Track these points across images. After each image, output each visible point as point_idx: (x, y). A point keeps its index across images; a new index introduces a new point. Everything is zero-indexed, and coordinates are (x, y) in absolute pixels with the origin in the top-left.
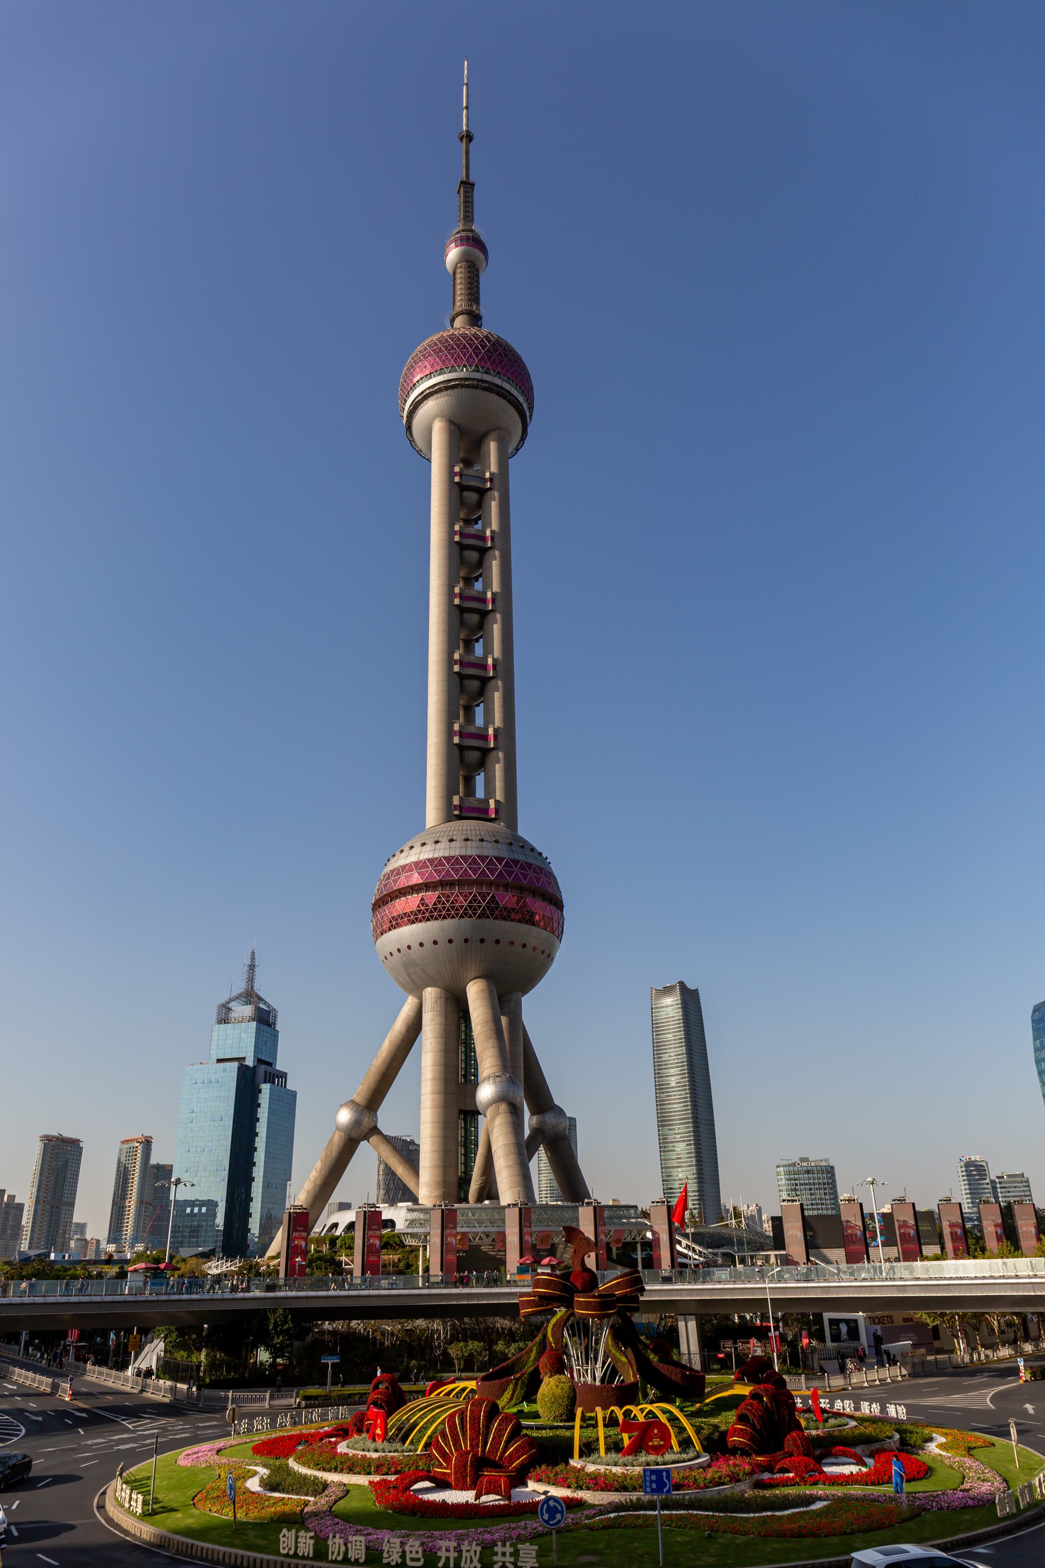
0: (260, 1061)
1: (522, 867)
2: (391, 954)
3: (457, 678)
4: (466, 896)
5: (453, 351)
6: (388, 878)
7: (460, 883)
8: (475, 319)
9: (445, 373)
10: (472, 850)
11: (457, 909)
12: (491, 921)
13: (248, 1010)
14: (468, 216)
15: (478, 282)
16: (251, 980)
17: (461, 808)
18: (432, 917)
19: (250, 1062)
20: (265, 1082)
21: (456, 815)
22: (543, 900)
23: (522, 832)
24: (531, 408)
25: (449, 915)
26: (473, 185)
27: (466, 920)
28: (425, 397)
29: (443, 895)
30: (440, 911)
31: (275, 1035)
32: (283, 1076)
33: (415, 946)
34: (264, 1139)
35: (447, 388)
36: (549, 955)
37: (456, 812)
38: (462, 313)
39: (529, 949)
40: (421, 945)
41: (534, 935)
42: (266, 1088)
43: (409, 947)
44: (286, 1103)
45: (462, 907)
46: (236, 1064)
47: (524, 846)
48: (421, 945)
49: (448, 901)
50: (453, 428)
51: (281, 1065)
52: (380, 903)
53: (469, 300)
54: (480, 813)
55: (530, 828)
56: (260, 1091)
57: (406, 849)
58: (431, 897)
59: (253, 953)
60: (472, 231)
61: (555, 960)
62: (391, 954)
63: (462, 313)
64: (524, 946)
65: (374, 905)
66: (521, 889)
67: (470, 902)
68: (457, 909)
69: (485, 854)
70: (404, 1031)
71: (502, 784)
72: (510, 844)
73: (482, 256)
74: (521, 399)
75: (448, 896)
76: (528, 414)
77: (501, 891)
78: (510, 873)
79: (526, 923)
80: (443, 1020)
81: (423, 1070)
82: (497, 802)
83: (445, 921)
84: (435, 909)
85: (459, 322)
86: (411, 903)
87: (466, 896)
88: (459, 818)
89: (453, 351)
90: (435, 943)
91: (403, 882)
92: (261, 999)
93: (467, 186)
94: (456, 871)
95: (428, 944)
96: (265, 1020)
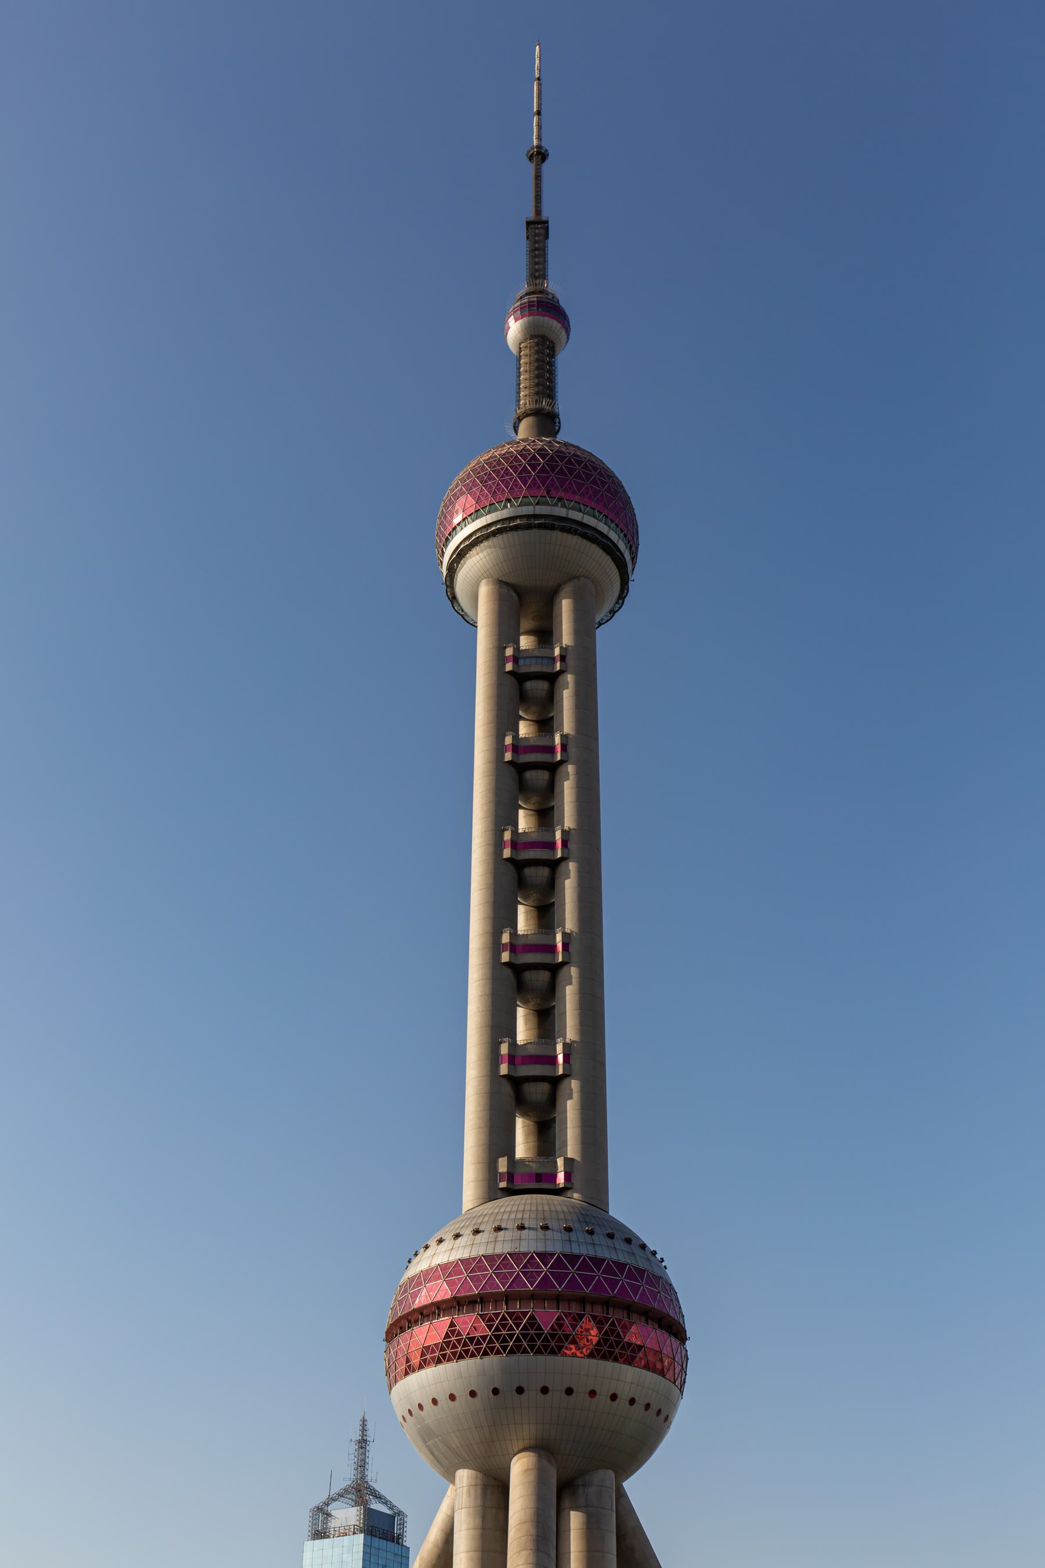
1: (609, 1270)
5: (505, 477)
6: (405, 1291)
7: (507, 1298)
8: (547, 421)
9: (496, 510)
10: (503, 1246)
11: (505, 1340)
12: (529, 1360)
15: (551, 364)
17: (510, 1176)
21: (502, 1189)
23: (619, 1209)
27: (492, 1360)
28: (461, 554)
35: (487, 537)
37: (503, 1185)
38: (526, 415)
48: (452, 1397)
50: (505, 590)
54: (541, 1182)
55: (622, 1207)
57: (433, 1243)
58: (468, 1322)
60: (542, 292)
63: (526, 415)
67: (497, 1329)
69: (550, 1249)
70: (440, 1545)
71: (578, 1131)
72: (569, 1229)
73: (556, 324)
78: (587, 1281)
80: (478, 1521)
82: (569, 1162)
83: (486, 1359)
85: (525, 429)
86: (429, 1333)
88: (510, 1192)
89: (505, 477)
90: (452, 1397)
91: (423, 1299)
94: (503, 1278)
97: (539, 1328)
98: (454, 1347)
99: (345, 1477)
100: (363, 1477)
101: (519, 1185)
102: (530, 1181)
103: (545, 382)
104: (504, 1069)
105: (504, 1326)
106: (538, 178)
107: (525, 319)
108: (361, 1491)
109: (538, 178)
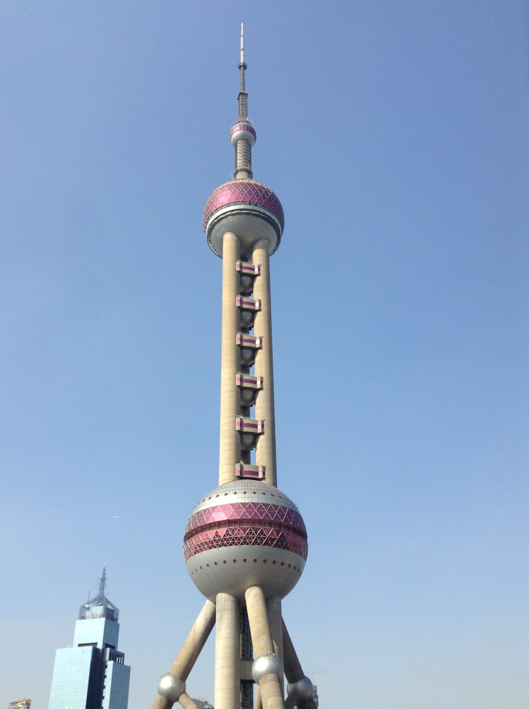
0: (106, 645)
2: (196, 570)
3: (238, 388)
4: (245, 530)
11: (239, 539)
13: (99, 610)
14: (245, 114)
16: (102, 588)
18: (223, 544)
19: (100, 646)
20: (110, 660)
22: (294, 532)
25: (234, 543)
29: (230, 529)
30: (228, 540)
31: (117, 627)
32: (122, 655)
33: (212, 565)
34: (109, 701)
36: (299, 570)
38: (241, 170)
39: (285, 566)
40: (216, 563)
41: (289, 556)
42: (110, 664)
43: (208, 565)
44: (123, 675)
45: (242, 538)
46: (90, 648)
47: (281, 496)
49: (233, 534)
51: (120, 649)
52: (189, 536)
53: (245, 162)
56: (106, 667)
59: (104, 570)
61: (303, 574)
62: (196, 570)
63: (241, 170)
64: (282, 564)
65: (185, 537)
66: (280, 525)
67: (248, 534)
68: (239, 539)
73: (252, 136)
75: (233, 531)
77: (267, 527)
79: (284, 548)
81: (216, 651)
84: (225, 539)
87: (245, 530)
92: (108, 602)
95: (220, 563)
96: (111, 616)
97: (265, 535)
98: (217, 542)
99: (95, 594)
100: (103, 593)
102: (249, 474)
103: (248, 159)
104: (238, 428)
105: (251, 533)
106: (244, 75)
107: (241, 131)
109: (244, 75)
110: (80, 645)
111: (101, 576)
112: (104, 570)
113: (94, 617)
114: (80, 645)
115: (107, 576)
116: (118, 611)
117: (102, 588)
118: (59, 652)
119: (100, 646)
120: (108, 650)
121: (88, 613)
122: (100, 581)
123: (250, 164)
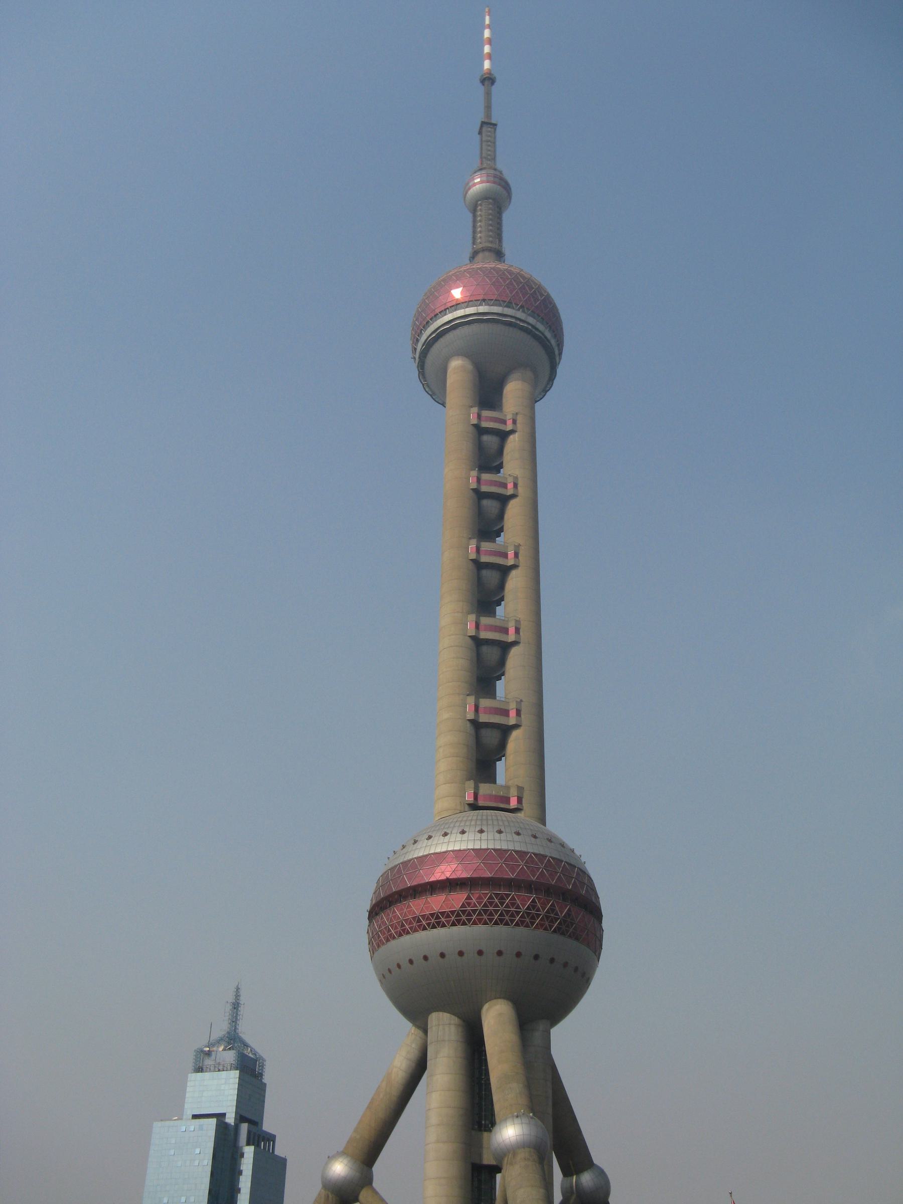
24: (560, 345)
26: (495, 125)
38: (483, 250)
60: (495, 170)
74: (548, 334)
76: (557, 352)
93: (488, 125)
99: (221, 1028)
100: (236, 1029)
101: (481, 803)
108: (233, 1039)
110: (195, 1117)
111: (231, 998)
112: (238, 989)
113: (219, 1068)
114: (195, 1117)
115: (242, 1000)
116: (264, 1060)
117: (234, 1020)
118: (157, 1125)
119: (230, 1119)
120: (244, 1127)
121: (208, 1062)
122: (229, 1007)
123: (500, 240)
